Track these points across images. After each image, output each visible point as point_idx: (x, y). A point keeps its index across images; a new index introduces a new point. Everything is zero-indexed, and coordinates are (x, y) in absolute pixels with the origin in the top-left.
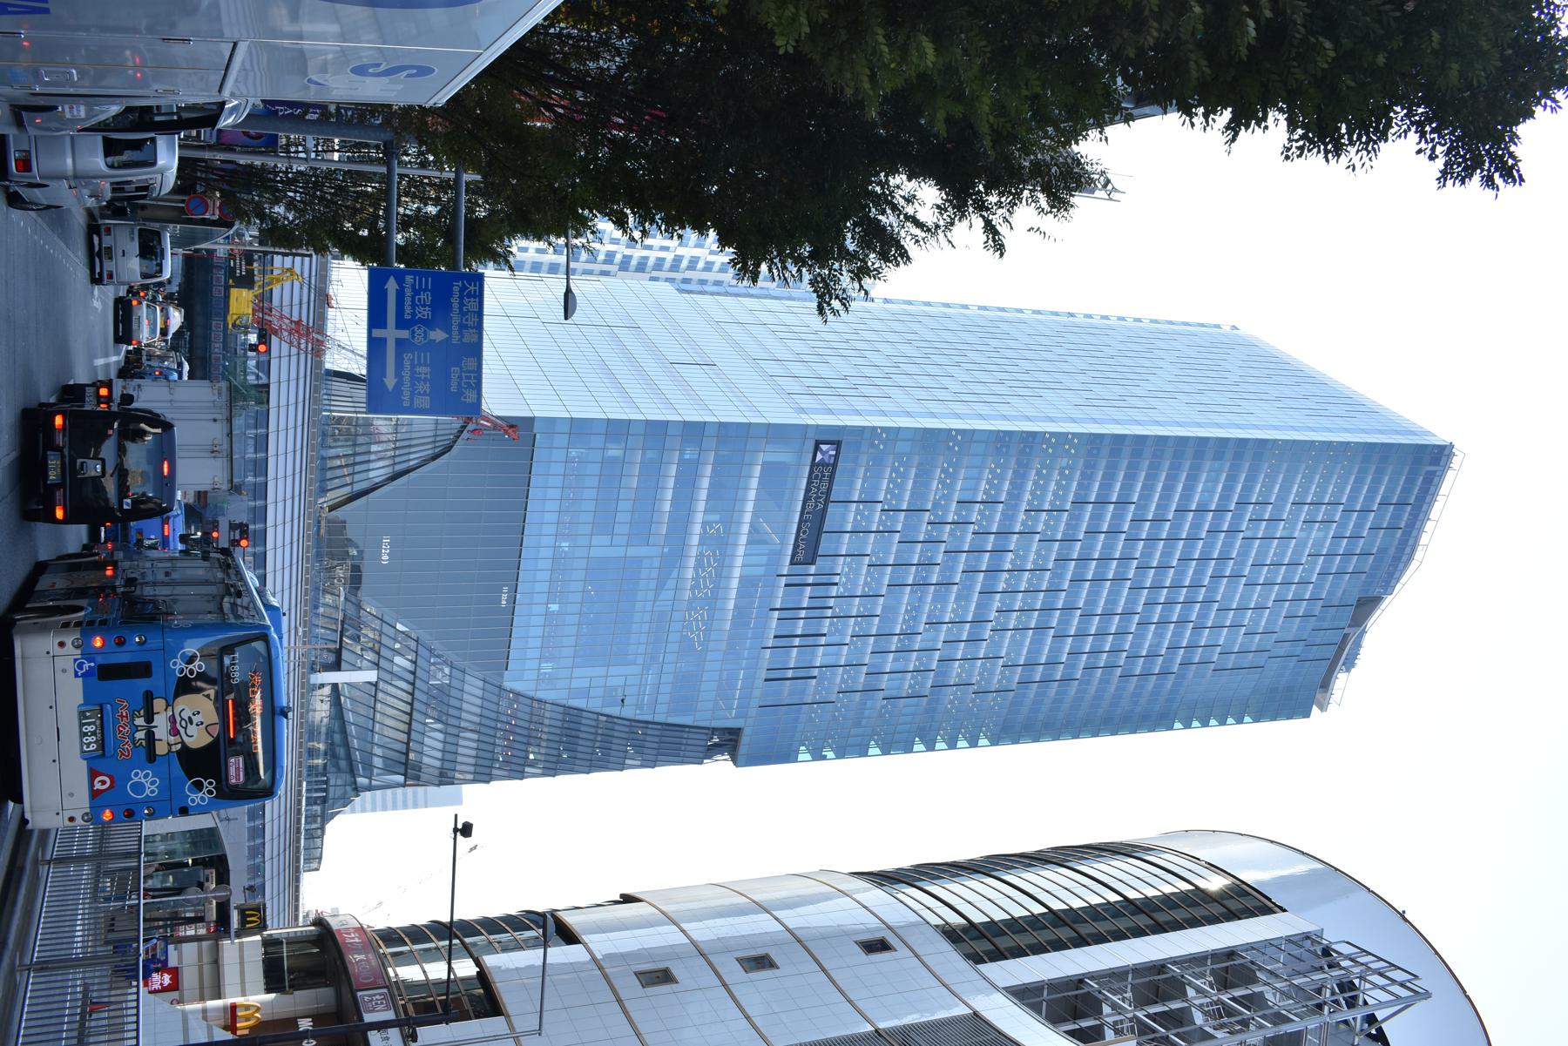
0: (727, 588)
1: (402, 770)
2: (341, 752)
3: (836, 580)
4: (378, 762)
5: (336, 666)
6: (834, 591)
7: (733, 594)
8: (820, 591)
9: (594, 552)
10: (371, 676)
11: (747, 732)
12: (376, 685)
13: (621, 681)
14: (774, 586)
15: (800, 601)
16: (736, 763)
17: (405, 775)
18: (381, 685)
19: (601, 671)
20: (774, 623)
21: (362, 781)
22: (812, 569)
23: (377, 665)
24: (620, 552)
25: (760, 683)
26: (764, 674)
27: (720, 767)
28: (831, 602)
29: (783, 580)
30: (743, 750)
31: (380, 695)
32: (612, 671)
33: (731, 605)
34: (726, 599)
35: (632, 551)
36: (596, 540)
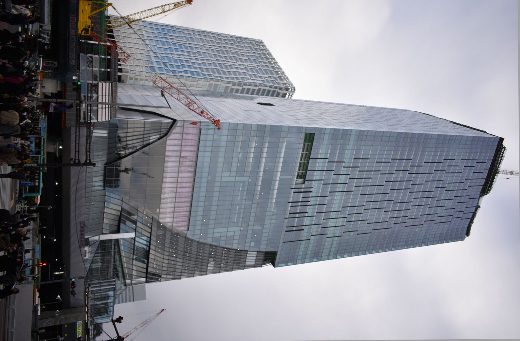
0: (273, 194)
1: (145, 275)
2: (119, 269)
3: (312, 190)
4: (134, 273)
5: (118, 231)
6: (311, 194)
7: (275, 196)
8: (307, 194)
9: (224, 179)
10: (132, 235)
11: (278, 253)
12: (134, 239)
13: (232, 234)
14: (290, 193)
15: (299, 199)
16: (274, 266)
17: (146, 278)
18: (137, 239)
19: (225, 230)
20: (289, 208)
21: (128, 281)
22: (303, 186)
23: (135, 230)
24: (233, 179)
25: (283, 233)
26: (285, 229)
27: (269, 267)
28: (310, 199)
29: (293, 190)
30: (277, 260)
31: (136, 244)
32: (230, 229)
33: (274, 201)
34: (272, 198)
35: (238, 179)
36: (225, 174)
